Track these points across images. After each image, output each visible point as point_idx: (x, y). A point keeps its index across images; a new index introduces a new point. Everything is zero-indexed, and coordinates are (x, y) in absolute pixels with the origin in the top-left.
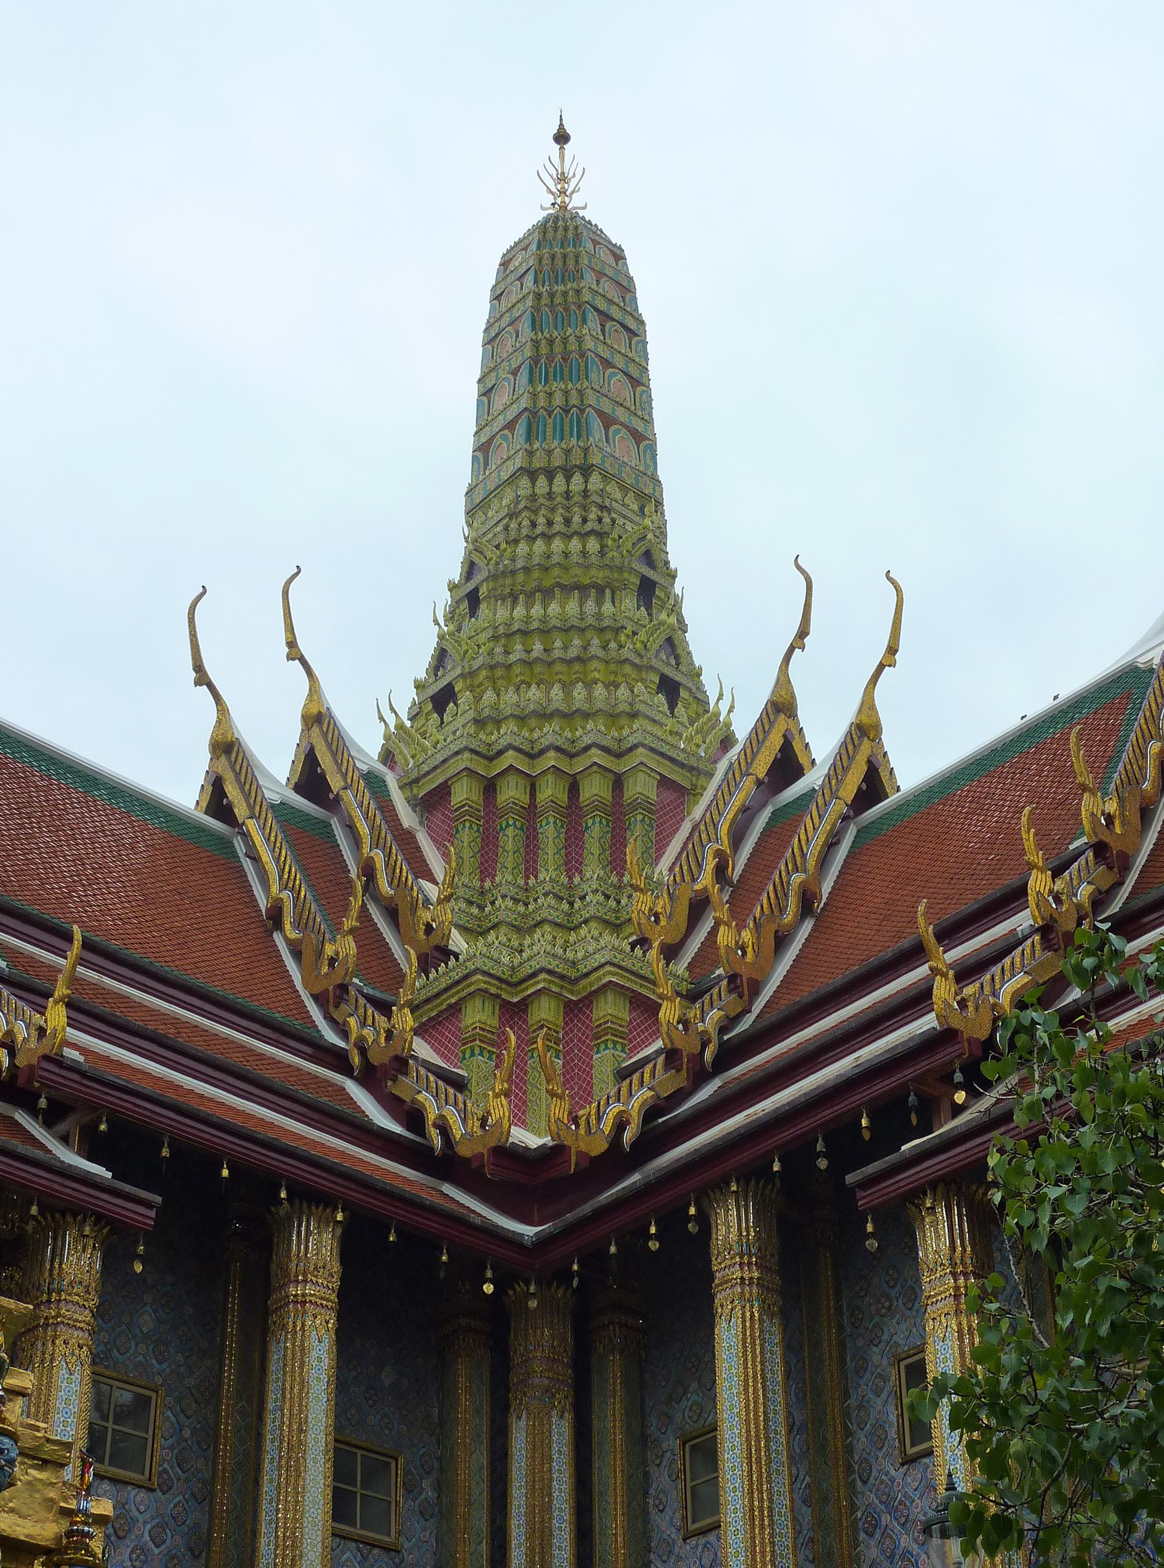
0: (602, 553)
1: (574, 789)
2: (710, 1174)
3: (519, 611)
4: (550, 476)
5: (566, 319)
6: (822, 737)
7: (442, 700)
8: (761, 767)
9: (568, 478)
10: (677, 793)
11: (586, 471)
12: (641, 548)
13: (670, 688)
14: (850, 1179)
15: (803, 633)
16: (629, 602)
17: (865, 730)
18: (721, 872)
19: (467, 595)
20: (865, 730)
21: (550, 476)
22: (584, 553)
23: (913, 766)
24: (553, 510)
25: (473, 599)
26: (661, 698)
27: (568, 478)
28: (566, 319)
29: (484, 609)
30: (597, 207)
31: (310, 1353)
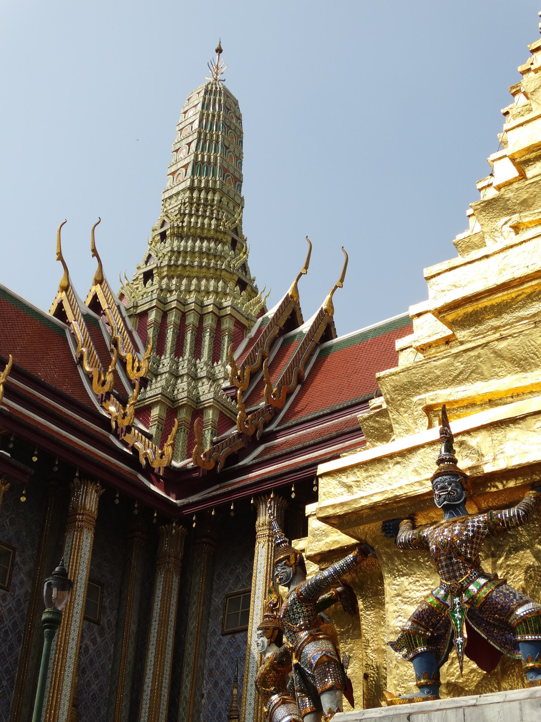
0: (218, 226)
4: (200, 191)
5: (222, 127)
7: (148, 276)
8: (282, 323)
9: (207, 193)
10: (241, 328)
12: (234, 226)
13: (243, 284)
19: (160, 234)
21: (200, 191)
25: (163, 236)
26: (238, 288)
27: (207, 193)
28: (222, 127)
29: (168, 241)
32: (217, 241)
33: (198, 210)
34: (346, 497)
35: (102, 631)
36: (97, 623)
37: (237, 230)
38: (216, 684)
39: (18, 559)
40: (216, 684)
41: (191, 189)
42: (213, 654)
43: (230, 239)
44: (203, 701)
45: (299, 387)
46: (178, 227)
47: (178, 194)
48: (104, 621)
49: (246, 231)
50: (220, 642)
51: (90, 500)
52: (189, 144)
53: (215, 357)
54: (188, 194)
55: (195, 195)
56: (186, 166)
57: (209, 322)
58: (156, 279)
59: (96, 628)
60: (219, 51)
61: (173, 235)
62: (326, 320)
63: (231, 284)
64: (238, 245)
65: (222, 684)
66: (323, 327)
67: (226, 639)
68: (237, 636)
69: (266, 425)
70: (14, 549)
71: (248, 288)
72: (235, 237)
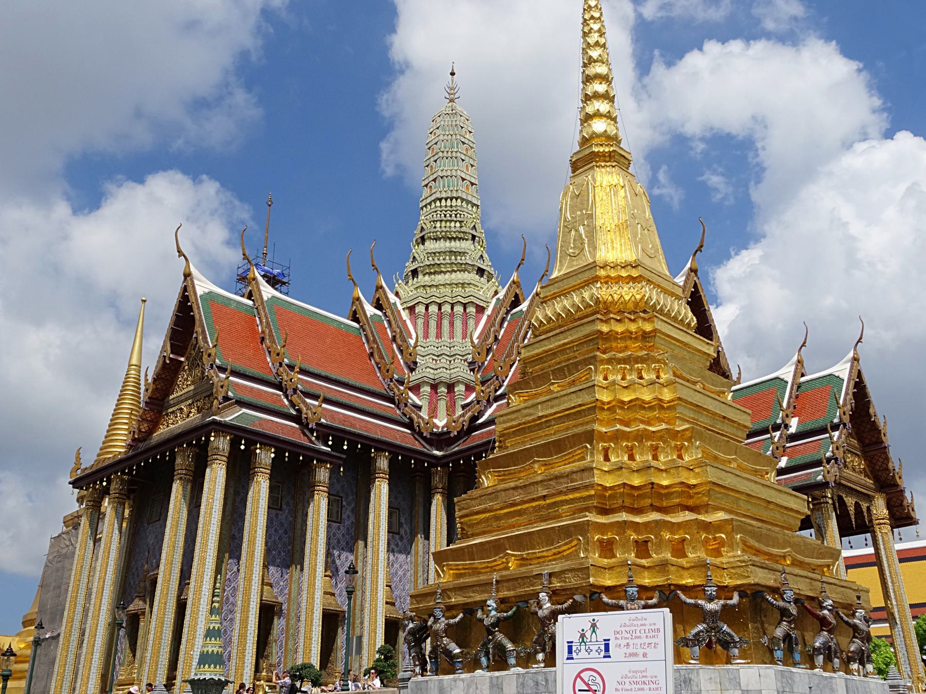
4: (446, 199)
8: (507, 304)
18: (496, 338)
21: (446, 199)
31: (381, 491)
35: (401, 538)
36: (398, 534)
39: (344, 503)
47: (430, 204)
48: (402, 532)
51: (383, 463)
58: (420, 276)
59: (397, 537)
60: (453, 74)
61: (430, 238)
69: (496, 391)
70: (341, 497)
72: (475, 233)
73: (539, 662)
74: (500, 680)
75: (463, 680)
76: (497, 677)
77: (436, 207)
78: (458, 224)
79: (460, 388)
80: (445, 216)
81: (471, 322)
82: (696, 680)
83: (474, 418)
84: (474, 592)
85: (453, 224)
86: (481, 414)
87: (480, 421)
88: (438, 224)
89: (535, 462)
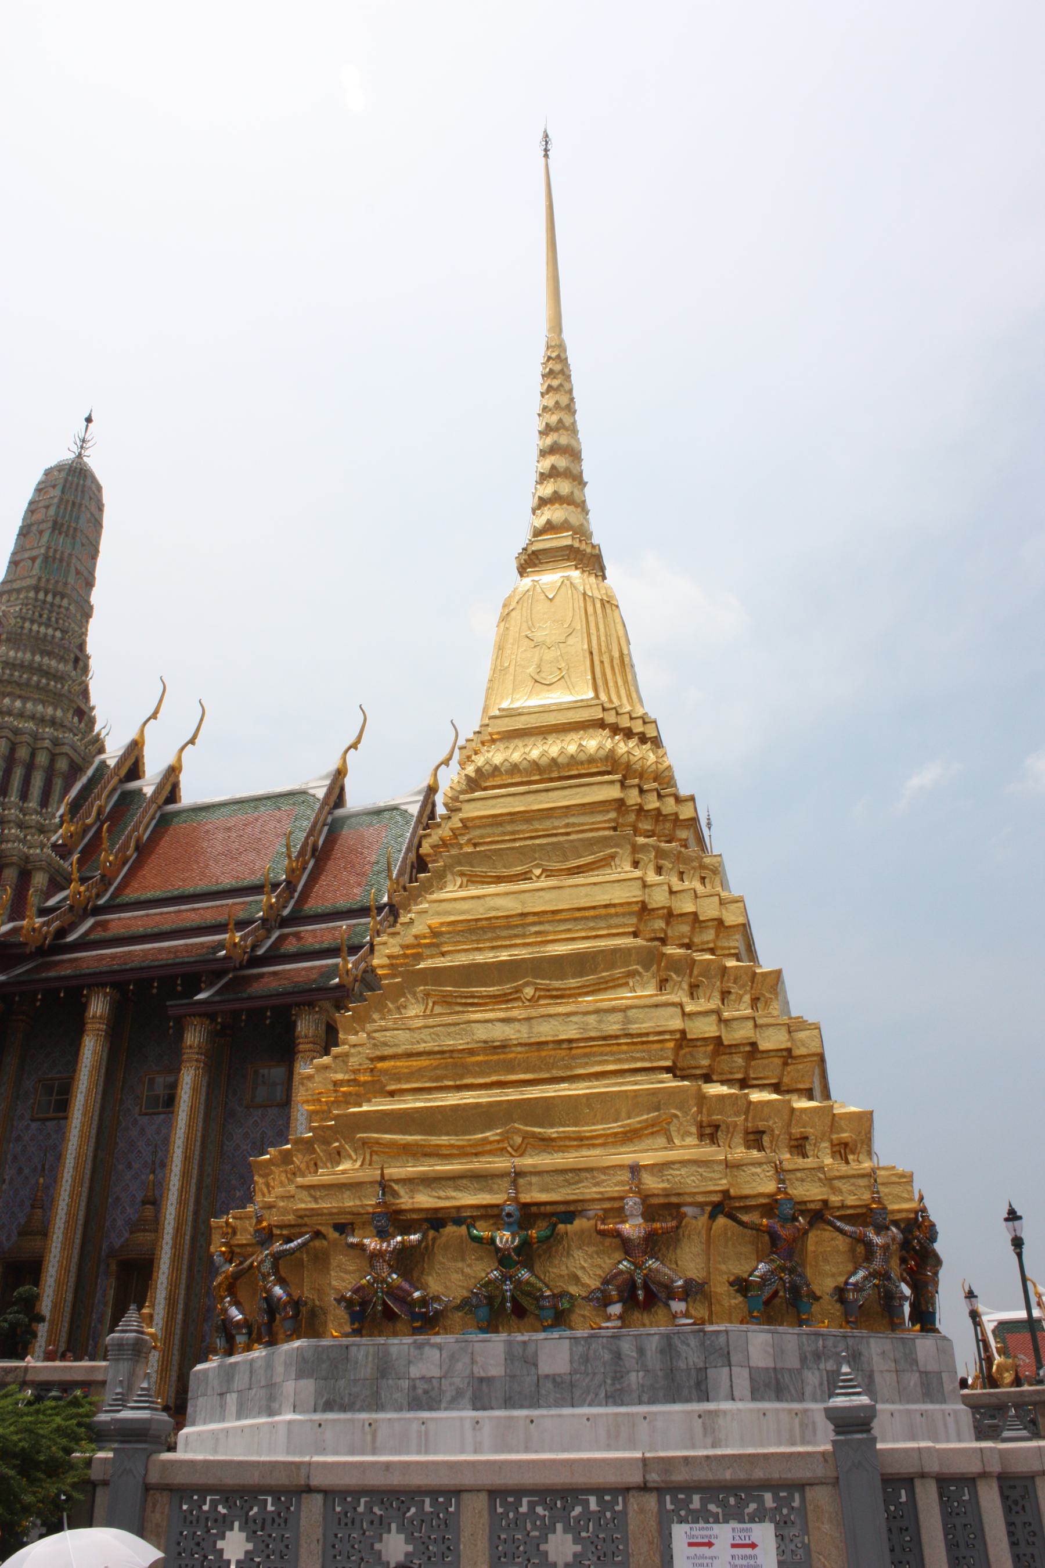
0: (62, 639)
1: (33, 755)
2: (97, 980)
3: (20, 654)
6: (153, 769)
8: (123, 772)
11: (63, 596)
14: (168, 1003)
15: (154, 716)
16: (70, 666)
17: (173, 772)
20: (173, 772)
22: (53, 636)
23: (189, 795)
24: (42, 609)
26: (76, 719)
27: (54, 596)
30: (94, 462)
32: (62, 659)
33: (41, 616)
34: (315, 1206)
37: (82, 646)
38: (20, 1171)
40: (20, 1171)
41: (37, 589)
42: (19, 1138)
43: (72, 656)
44: (4, 1187)
45: (135, 855)
46: (16, 634)
47: (18, 591)
49: (90, 649)
50: (27, 1128)
52: (41, 532)
53: (44, 802)
54: (32, 594)
55: (41, 595)
56: (33, 559)
57: (42, 759)
60: (89, 420)
62: (172, 779)
63: (70, 715)
64: (81, 664)
65: (26, 1171)
66: (168, 788)
67: (34, 1125)
68: (48, 1123)
69: (98, 896)
71: (86, 717)
73: (608, 1318)
74: (531, 1349)
75: (439, 1347)
76: (524, 1342)
77: (27, 598)
78: (58, 634)
79: (40, 879)
80: (41, 616)
81: (58, 783)
82: (866, 1353)
83: (62, 933)
84: (457, 1188)
85: (50, 631)
86: (73, 926)
87: (71, 938)
88: (27, 625)
89: (527, 984)
